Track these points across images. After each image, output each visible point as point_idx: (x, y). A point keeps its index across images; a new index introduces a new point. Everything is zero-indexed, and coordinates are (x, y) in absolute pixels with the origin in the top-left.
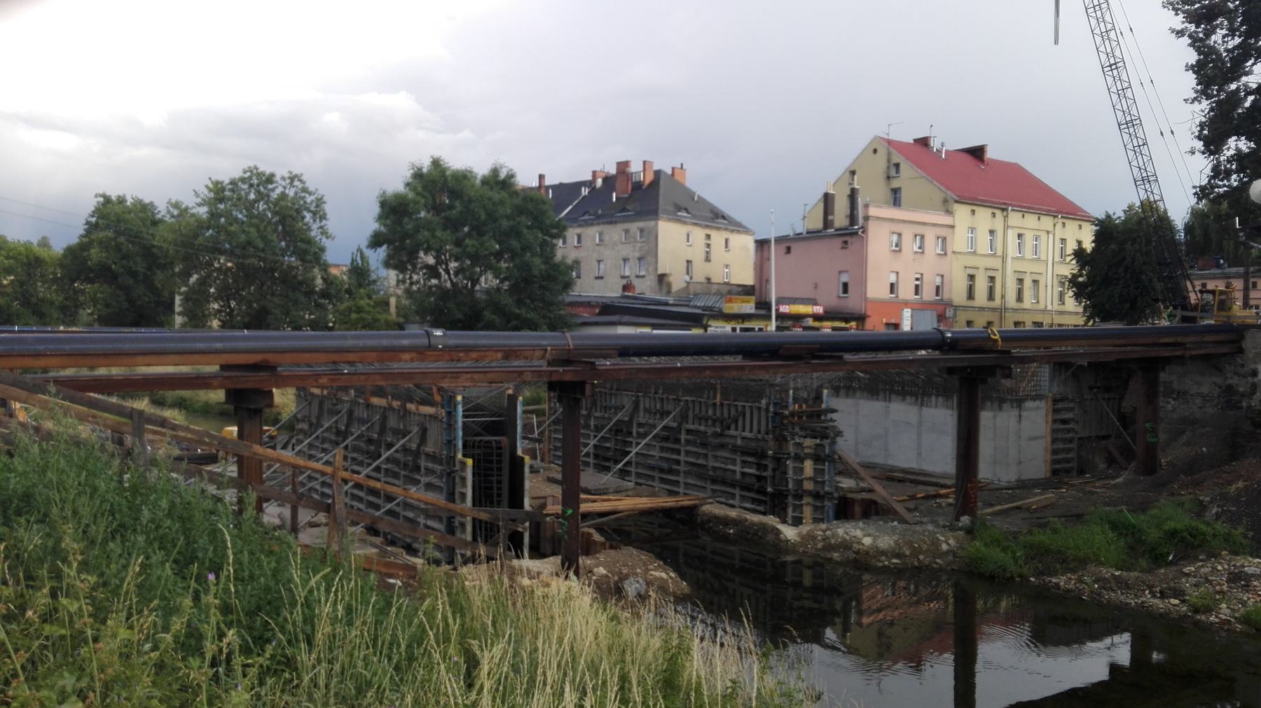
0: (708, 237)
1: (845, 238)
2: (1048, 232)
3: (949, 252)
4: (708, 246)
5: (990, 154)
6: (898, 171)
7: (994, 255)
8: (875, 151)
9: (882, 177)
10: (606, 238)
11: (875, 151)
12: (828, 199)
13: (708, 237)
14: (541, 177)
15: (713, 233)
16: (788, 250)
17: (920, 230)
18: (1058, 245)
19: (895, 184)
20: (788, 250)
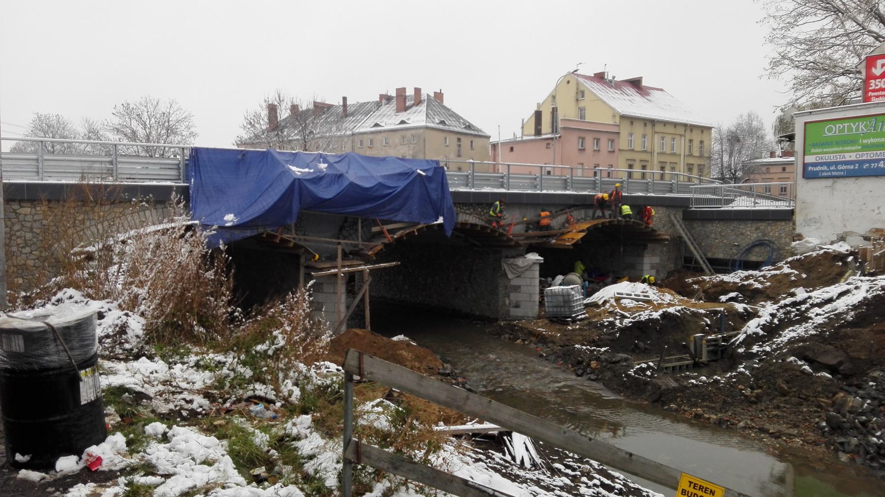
0: (459, 140)
1: (548, 142)
2: (681, 135)
3: (616, 150)
4: (459, 146)
5: (644, 83)
6: (583, 96)
7: (646, 152)
8: (568, 82)
9: (573, 100)
10: (391, 142)
11: (568, 82)
12: (538, 115)
13: (459, 140)
14: (345, 99)
15: (463, 138)
16: (512, 149)
17: (597, 136)
18: (688, 144)
19: (582, 104)
20: (512, 149)
